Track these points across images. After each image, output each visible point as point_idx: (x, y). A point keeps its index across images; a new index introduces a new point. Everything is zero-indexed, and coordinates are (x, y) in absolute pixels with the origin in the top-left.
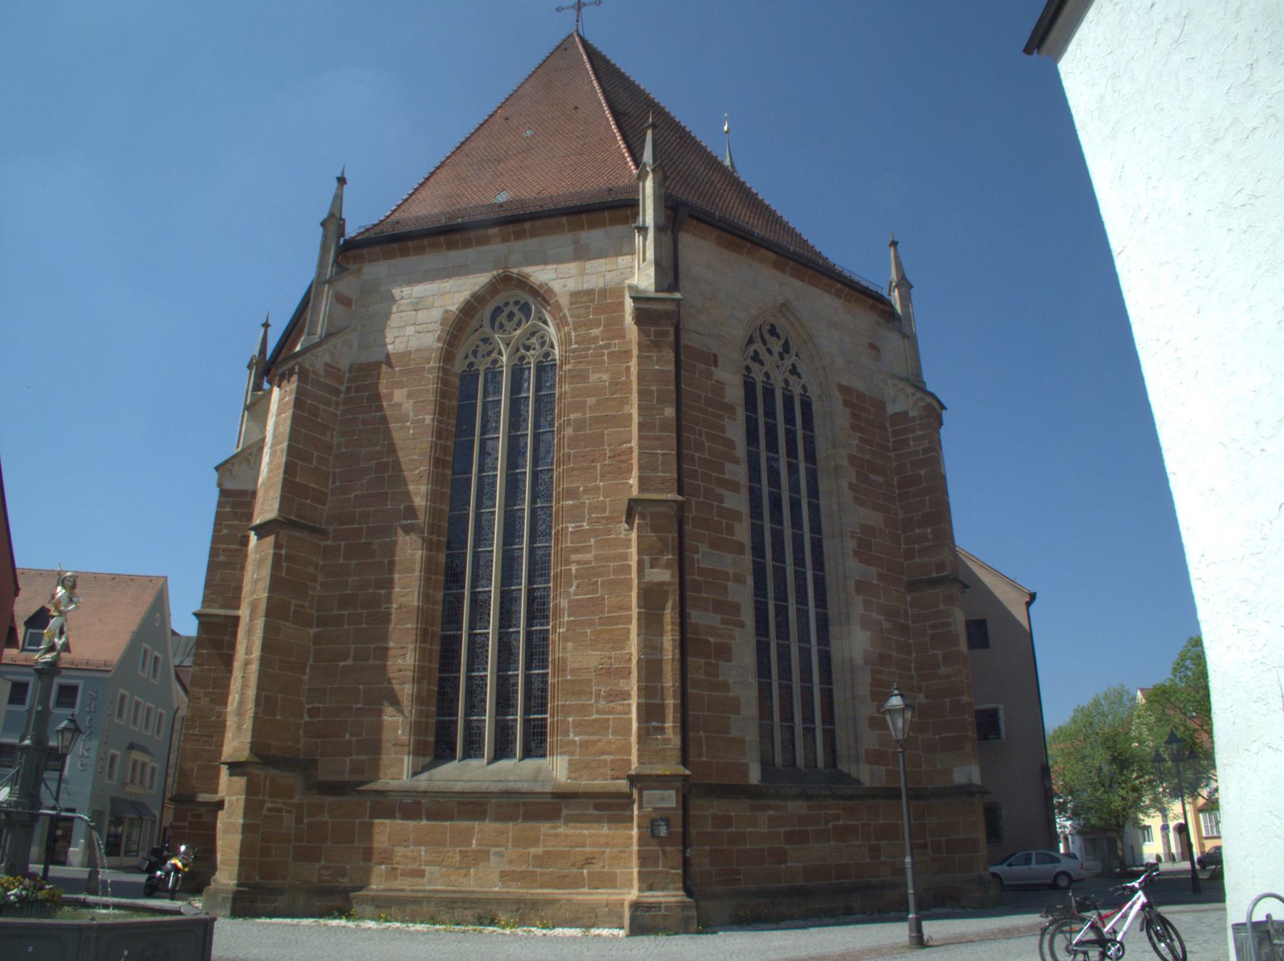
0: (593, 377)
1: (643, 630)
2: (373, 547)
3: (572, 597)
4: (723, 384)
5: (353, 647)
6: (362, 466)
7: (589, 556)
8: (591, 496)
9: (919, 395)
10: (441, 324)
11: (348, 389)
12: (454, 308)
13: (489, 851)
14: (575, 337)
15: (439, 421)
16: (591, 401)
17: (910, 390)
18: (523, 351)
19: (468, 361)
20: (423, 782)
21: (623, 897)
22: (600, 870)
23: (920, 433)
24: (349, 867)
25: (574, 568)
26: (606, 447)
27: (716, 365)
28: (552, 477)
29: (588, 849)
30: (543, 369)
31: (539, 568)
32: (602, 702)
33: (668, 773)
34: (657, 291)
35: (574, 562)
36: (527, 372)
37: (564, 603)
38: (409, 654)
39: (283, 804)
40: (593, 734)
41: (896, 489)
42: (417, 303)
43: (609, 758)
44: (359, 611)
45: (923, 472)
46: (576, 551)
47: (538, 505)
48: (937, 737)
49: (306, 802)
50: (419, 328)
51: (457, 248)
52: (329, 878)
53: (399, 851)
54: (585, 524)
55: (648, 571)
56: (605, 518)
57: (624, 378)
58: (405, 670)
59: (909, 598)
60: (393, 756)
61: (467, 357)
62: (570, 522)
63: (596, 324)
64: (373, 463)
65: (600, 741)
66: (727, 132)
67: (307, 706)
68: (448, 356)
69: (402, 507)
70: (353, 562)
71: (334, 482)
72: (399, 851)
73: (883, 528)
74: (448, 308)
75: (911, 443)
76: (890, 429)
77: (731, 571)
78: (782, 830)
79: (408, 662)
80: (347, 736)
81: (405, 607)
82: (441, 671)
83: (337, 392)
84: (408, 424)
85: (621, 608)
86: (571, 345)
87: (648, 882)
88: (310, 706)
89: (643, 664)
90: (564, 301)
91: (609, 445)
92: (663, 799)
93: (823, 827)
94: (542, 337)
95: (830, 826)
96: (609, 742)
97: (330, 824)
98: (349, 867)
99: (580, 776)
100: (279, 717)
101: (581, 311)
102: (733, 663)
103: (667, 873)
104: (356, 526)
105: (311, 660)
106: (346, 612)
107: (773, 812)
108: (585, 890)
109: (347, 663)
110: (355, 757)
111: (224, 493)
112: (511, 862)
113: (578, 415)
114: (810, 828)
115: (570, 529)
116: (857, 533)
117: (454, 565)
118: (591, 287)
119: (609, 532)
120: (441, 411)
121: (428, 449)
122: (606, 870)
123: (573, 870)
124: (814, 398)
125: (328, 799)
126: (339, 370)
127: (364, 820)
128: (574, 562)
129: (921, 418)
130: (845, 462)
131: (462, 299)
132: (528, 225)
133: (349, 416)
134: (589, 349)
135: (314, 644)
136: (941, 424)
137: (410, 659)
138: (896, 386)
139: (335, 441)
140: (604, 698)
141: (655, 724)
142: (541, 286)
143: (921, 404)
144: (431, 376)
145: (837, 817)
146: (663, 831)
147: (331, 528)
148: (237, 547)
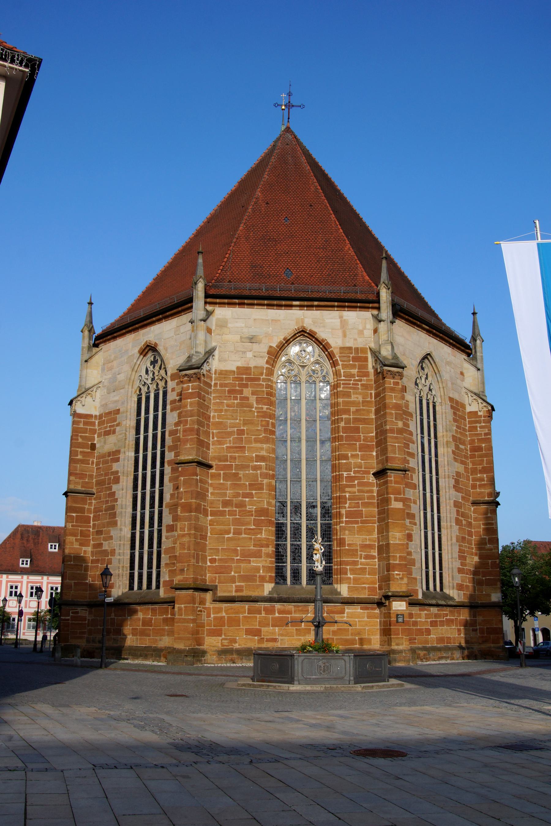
2: (240, 476)
3: (347, 509)
4: (408, 402)
5: (232, 527)
6: (228, 430)
7: (355, 489)
8: (356, 459)
9: (485, 404)
10: (268, 354)
11: (216, 384)
12: (274, 345)
14: (344, 372)
16: (353, 409)
17: (480, 401)
23: (484, 424)
24: (237, 638)
25: (347, 495)
26: (361, 434)
27: (406, 392)
29: (357, 627)
32: (363, 560)
37: (343, 511)
38: (263, 532)
39: (203, 608)
40: (359, 574)
41: (469, 452)
42: (252, 338)
43: (367, 586)
44: (234, 509)
45: (483, 445)
49: (211, 607)
50: (255, 354)
52: (227, 644)
53: (263, 629)
54: (352, 473)
58: (263, 540)
59: (472, 509)
60: (258, 583)
63: (353, 367)
64: (236, 429)
69: (254, 455)
70: (229, 483)
71: (213, 438)
72: (263, 629)
73: (464, 473)
74: (272, 345)
75: (478, 429)
76: (467, 420)
78: (429, 620)
80: (233, 573)
84: (254, 409)
88: (210, 558)
90: (336, 352)
91: (362, 433)
92: (401, 606)
93: (442, 619)
95: (445, 619)
97: (226, 618)
98: (237, 638)
100: (200, 564)
101: (345, 359)
102: (413, 542)
104: (229, 463)
106: (227, 509)
107: (426, 612)
110: (237, 584)
113: (347, 416)
114: (438, 620)
115: (345, 475)
116: (454, 476)
124: (437, 404)
125: (224, 605)
127: (245, 615)
129: (484, 417)
131: (279, 341)
132: (316, 303)
133: (218, 401)
134: (351, 380)
137: (264, 535)
138: (472, 397)
140: (364, 558)
142: (323, 340)
144: (264, 383)
145: (447, 615)
146: (400, 620)
147: (213, 463)
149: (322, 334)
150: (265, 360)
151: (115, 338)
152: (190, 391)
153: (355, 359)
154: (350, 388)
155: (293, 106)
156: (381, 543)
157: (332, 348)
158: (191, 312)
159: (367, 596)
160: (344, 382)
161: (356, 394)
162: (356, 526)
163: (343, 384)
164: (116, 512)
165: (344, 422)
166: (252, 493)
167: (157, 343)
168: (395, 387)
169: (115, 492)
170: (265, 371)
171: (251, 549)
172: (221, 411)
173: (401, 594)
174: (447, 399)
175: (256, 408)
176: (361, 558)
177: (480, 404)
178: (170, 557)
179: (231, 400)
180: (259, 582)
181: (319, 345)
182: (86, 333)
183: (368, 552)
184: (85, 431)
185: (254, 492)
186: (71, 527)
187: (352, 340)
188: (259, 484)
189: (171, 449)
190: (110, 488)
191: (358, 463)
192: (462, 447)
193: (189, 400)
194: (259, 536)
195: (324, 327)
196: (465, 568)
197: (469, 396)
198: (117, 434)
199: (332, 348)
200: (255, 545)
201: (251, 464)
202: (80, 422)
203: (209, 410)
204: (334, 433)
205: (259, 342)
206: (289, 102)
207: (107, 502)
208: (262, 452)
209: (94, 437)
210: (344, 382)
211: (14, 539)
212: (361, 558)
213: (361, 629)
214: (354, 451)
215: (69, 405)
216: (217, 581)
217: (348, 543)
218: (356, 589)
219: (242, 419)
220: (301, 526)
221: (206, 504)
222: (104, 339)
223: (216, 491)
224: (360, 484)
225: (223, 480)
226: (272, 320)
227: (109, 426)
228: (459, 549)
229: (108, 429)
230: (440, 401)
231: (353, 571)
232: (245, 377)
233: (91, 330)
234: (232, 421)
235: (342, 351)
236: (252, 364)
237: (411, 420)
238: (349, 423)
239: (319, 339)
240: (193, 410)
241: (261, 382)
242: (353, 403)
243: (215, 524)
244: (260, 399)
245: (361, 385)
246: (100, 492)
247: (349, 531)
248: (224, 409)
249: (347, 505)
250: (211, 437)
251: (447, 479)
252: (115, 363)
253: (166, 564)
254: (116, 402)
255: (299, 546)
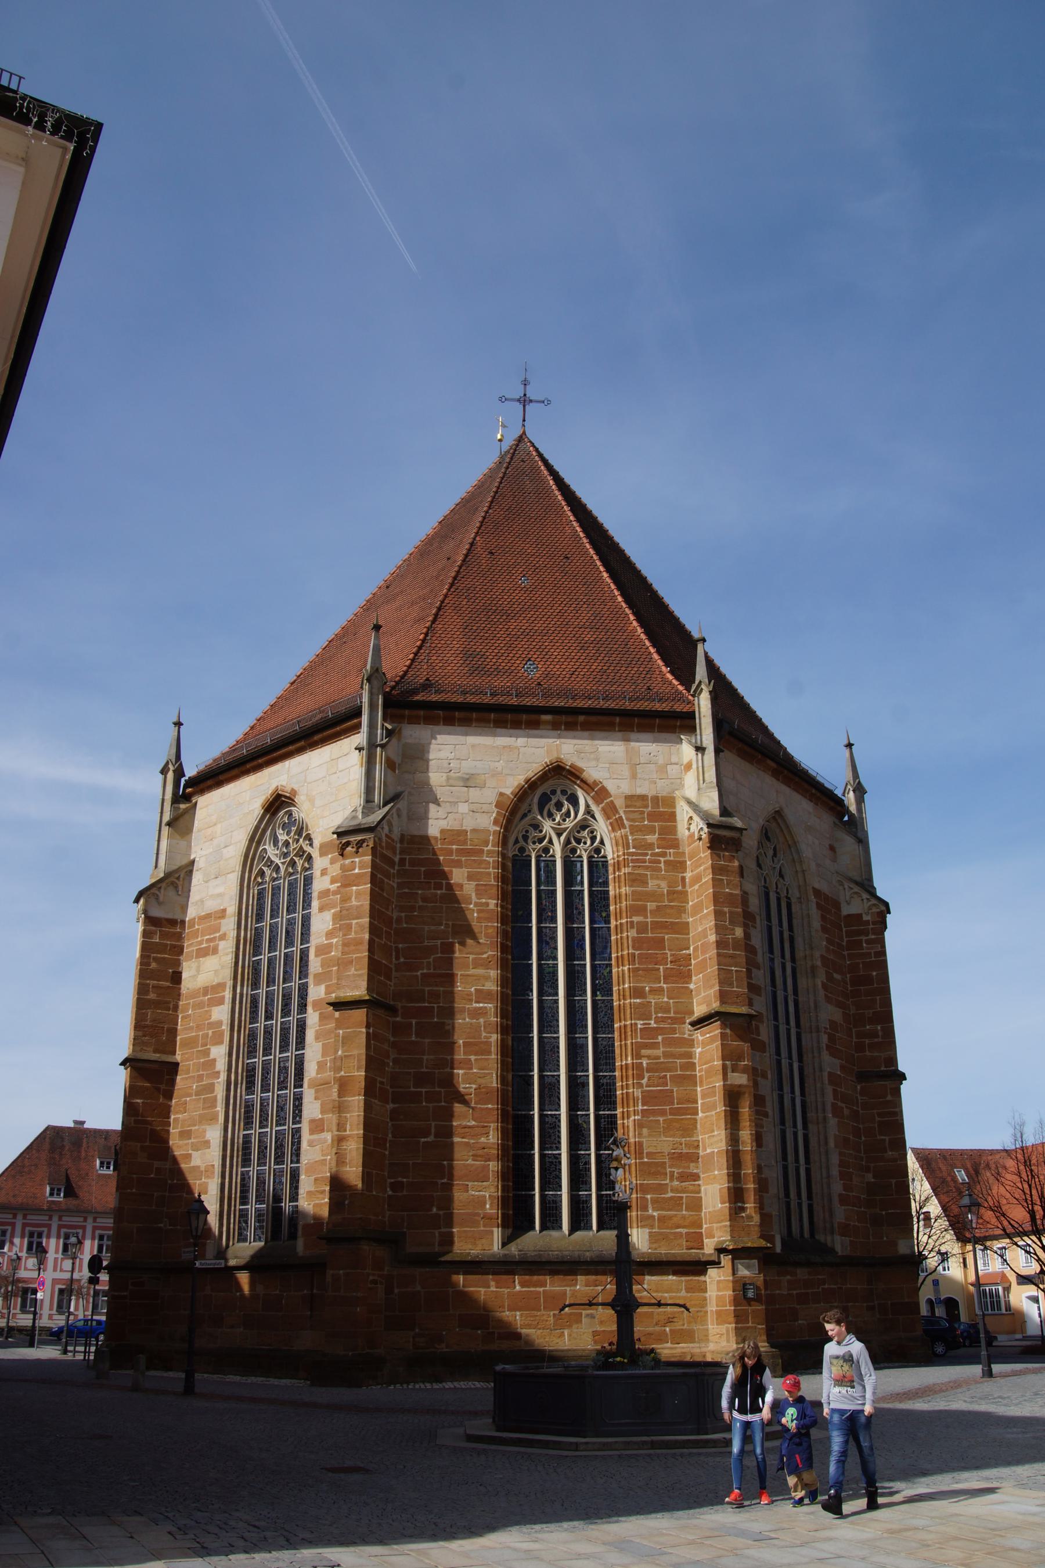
0: (652, 884)
1: (729, 1126)
3: (645, 1089)
5: (433, 1124)
6: (426, 944)
7: (659, 1052)
8: (656, 997)
9: (874, 901)
10: (496, 806)
11: (402, 861)
12: (508, 791)
13: (581, 1313)
14: (633, 840)
15: (502, 907)
16: (651, 906)
17: (865, 896)
18: (574, 844)
19: (518, 846)
20: (513, 1249)
21: (704, 1350)
22: (682, 1327)
23: (873, 937)
25: (645, 1062)
28: (611, 972)
30: (599, 867)
31: (605, 1057)
32: (676, 1183)
33: (755, 1245)
34: (721, 815)
35: (644, 1056)
36: (579, 865)
38: (491, 1133)
42: (468, 779)
43: (684, 1231)
44: (437, 1089)
45: (874, 973)
46: (646, 1046)
47: (599, 998)
48: (884, 1213)
50: (474, 807)
51: (506, 727)
54: (653, 1022)
55: (730, 1074)
56: (670, 1018)
57: (680, 888)
58: (490, 1148)
59: (859, 1087)
60: (482, 1229)
61: (517, 841)
62: (639, 1019)
63: (651, 830)
64: (439, 942)
65: (676, 1215)
66: (500, 440)
67: (389, 1181)
68: (504, 842)
69: (473, 989)
70: (427, 1041)
71: (397, 958)
76: (844, 929)
77: (759, 1068)
78: (795, 1292)
79: (492, 1141)
80: (435, 1210)
81: (484, 1088)
82: (514, 1149)
83: (391, 863)
84: (472, 906)
85: (688, 1101)
86: (628, 848)
87: (741, 1335)
88: (392, 1181)
89: (730, 1154)
90: (620, 803)
91: (670, 950)
94: (592, 832)
95: (820, 1290)
96: (684, 1217)
99: (660, 1247)
101: (636, 816)
103: (755, 1327)
105: (390, 1135)
106: (424, 1090)
107: (789, 1277)
108: (669, 1345)
109: (429, 1139)
111: (151, 921)
112: (601, 1322)
115: (639, 1026)
116: (826, 1028)
117: (520, 1048)
118: (644, 793)
119: (674, 1031)
120: (504, 896)
121: (495, 934)
122: (685, 1327)
123: (657, 1328)
124: (793, 900)
126: (393, 840)
128: (644, 1056)
129: (874, 923)
130: (819, 963)
131: (516, 784)
132: (581, 718)
133: (406, 890)
134: (646, 854)
135: (391, 1120)
136: (886, 928)
138: (852, 889)
139: (395, 915)
140: (678, 1179)
141: (740, 1204)
142: (596, 783)
143: (875, 910)
144: (491, 860)
146: (750, 1294)
147: (399, 1005)
148: (168, 984)
149: (593, 772)
150: (492, 818)
151: (219, 784)
152: (357, 871)
153: (652, 817)
154: (647, 868)
155: (531, 401)
156: (708, 1151)
157: (611, 796)
158: (359, 732)
159: (685, 1251)
160: (634, 857)
161: (657, 878)
162: (661, 1119)
163: (633, 861)
164: (216, 1096)
165: (635, 930)
166: (470, 1060)
167: (296, 789)
168: (728, 866)
169: (214, 1060)
170: (491, 838)
171: (468, 1164)
172: (412, 908)
173: (749, 1245)
174: (811, 893)
175: (476, 904)
176: (672, 1179)
177: (865, 901)
178: (316, 1180)
179: (430, 888)
180: (484, 1226)
181: (590, 790)
182: (170, 775)
183: (685, 1167)
184: (161, 948)
185: (473, 1058)
186: (133, 1125)
187: (647, 782)
188: (482, 1042)
189: (319, 979)
190: (207, 1053)
191: (664, 1005)
192: (835, 975)
193: (354, 888)
194: (483, 1139)
195: (597, 759)
196: (851, 1194)
197: (846, 887)
198: (221, 953)
199: (611, 796)
200: (475, 1157)
201: (467, 1006)
202: (155, 933)
203: (390, 908)
204: (620, 950)
205: (482, 786)
206: (525, 395)
207: (200, 1078)
208: (486, 984)
209: (179, 960)
210: (634, 857)
211: (38, 1151)
212: (672, 1179)
213: (675, 1313)
214: (655, 983)
215: (134, 902)
216: (405, 1224)
217: (649, 1150)
218: (665, 1237)
219: (450, 923)
220: (559, 1121)
221: (384, 1080)
222: (202, 786)
223: (402, 1056)
224: (668, 1042)
225: (416, 1037)
226: (504, 747)
227: (207, 940)
228: (841, 1161)
229: (204, 945)
230: (798, 896)
231: (658, 1204)
232: (457, 849)
233: (179, 773)
234: (433, 928)
235: (629, 803)
236: (468, 824)
237: (752, 926)
238: (645, 931)
239: (588, 782)
240: (362, 905)
241: (485, 858)
242: (653, 896)
243: (402, 1117)
244: (483, 888)
245: (665, 862)
246: (188, 1060)
247: (649, 1128)
248: (417, 905)
249: (644, 1081)
250: (394, 956)
251: (814, 1035)
252: (218, 828)
253: (309, 1193)
254: (220, 895)
255: (557, 1158)
